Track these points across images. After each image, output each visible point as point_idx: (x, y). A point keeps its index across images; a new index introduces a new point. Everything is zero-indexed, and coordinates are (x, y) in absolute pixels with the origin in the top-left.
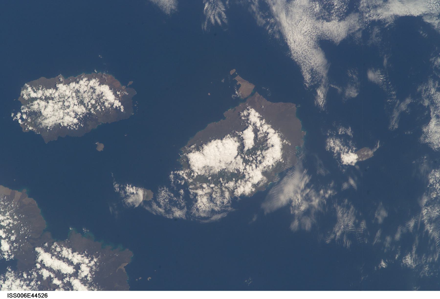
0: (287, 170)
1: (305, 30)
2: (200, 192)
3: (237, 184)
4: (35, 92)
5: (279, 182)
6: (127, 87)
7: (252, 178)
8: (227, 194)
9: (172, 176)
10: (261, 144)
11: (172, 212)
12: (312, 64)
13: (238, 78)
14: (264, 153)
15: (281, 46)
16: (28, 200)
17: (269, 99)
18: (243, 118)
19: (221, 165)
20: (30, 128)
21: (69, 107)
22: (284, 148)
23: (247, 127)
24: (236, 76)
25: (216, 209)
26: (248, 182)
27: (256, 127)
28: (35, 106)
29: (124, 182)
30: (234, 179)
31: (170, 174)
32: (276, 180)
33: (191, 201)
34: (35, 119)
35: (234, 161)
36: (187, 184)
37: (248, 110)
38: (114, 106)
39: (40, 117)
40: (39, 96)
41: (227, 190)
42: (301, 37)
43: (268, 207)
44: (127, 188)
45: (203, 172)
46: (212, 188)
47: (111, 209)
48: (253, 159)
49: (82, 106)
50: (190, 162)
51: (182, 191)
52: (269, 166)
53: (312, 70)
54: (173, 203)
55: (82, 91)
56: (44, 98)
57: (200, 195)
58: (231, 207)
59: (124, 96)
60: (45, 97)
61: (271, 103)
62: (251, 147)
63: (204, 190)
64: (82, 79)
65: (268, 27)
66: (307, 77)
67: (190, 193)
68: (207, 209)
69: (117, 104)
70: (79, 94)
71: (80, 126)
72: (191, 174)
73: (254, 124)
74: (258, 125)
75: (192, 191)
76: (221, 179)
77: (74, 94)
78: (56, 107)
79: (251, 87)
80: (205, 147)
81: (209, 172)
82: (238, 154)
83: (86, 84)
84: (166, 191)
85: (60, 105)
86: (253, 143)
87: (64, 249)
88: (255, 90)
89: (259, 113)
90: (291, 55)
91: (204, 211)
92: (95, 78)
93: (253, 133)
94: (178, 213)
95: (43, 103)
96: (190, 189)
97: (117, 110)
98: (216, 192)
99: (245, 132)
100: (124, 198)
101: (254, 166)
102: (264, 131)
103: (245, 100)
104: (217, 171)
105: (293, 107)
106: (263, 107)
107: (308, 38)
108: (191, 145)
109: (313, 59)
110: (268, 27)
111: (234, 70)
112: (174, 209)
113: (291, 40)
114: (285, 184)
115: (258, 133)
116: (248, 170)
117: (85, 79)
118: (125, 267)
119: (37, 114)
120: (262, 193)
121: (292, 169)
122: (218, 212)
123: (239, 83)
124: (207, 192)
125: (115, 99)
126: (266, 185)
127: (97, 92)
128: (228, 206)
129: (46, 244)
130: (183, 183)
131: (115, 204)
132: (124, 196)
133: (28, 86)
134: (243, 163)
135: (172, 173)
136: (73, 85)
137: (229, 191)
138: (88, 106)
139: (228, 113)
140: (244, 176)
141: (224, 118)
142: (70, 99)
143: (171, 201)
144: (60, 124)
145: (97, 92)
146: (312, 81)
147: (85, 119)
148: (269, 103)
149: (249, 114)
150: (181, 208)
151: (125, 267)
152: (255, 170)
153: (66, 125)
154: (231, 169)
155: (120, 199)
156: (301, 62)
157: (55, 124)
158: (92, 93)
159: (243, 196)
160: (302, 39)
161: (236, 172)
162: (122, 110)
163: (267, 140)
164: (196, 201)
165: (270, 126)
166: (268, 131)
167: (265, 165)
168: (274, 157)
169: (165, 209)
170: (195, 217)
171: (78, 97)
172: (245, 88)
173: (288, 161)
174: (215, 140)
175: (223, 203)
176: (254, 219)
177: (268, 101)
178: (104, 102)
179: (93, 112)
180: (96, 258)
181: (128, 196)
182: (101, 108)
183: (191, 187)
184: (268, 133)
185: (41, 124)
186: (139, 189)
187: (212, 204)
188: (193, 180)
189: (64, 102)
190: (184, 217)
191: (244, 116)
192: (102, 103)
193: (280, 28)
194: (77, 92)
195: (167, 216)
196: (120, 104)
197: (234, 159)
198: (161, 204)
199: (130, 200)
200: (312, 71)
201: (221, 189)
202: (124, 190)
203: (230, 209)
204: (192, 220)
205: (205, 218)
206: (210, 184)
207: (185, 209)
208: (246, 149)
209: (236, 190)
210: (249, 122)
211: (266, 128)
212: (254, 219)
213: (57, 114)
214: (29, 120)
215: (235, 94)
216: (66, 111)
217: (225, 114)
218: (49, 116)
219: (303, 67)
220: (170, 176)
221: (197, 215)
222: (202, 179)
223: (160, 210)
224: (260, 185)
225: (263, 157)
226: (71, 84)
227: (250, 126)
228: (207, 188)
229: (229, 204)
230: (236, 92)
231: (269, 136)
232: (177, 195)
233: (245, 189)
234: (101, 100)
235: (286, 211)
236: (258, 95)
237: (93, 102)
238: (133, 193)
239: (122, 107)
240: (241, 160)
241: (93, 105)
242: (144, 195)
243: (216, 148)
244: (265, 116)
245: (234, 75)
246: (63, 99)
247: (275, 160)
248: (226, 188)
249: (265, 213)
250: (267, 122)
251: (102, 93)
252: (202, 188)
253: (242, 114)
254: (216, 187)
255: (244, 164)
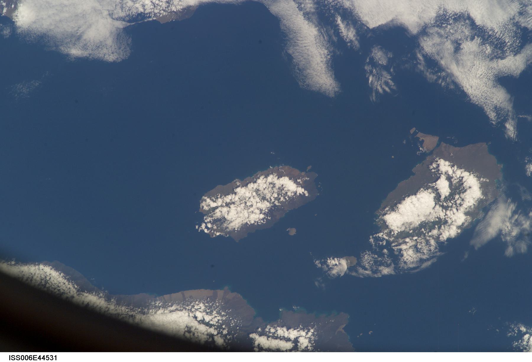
0: (490, 205)
1: (480, 73)
2: (404, 247)
3: (441, 230)
4: (214, 202)
5: (484, 218)
6: (306, 172)
7: (455, 221)
8: (432, 242)
9: (372, 240)
10: (458, 188)
11: (380, 271)
12: (495, 103)
13: (420, 135)
14: (462, 196)
15: (458, 94)
16: (231, 295)
17: (455, 146)
18: (433, 171)
19: (420, 218)
20: (218, 234)
21: (252, 206)
22: (484, 187)
23: (439, 178)
24: (417, 133)
25: (424, 257)
26: (451, 226)
27: (449, 175)
28: (218, 214)
29: (324, 255)
30: (437, 226)
31: (370, 238)
32: (481, 215)
33: (396, 257)
34: (221, 225)
35: (432, 211)
36: (389, 243)
37: (437, 161)
38: (298, 194)
39: (225, 222)
40: (220, 204)
41: (431, 238)
42: (478, 81)
43: (477, 243)
44: (329, 261)
45: (403, 229)
46: (416, 240)
47: (317, 284)
48: (452, 204)
49: (266, 202)
50: (387, 224)
51: (385, 251)
52: (471, 206)
53: (496, 108)
54: (379, 263)
55: (261, 188)
56: (224, 205)
57: (405, 250)
58: (439, 252)
59: (305, 182)
60: (226, 203)
61: (459, 148)
62: (447, 194)
63: (408, 244)
64: (259, 178)
65: (440, 81)
66: (492, 115)
67: (394, 250)
68: (415, 260)
69: (300, 190)
70: (259, 192)
71: (267, 219)
72: (391, 232)
73: (446, 173)
74: (450, 172)
75: (395, 248)
76: (423, 230)
77: (254, 194)
78: (239, 209)
79: (436, 139)
80: (400, 206)
81: (409, 227)
82: (436, 204)
83: (264, 181)
84: (369, 255)
85: (242, 206)
86: (449, 191)
87: (278, 328)
88: (440, 141)
89: (449, 161)
90: (470, 100)
91: (413, 262)
92: (272, 174)
93: (447, 181)
94: (386, 271)
95: (225, 210)
96: (394, 246)
97: (302, 196)
98: (421, 243)
99: (438, 182)
100: (327, 271)
101: (455, 210)
102: (458, 176)
103: (431, 153)
104: (418, 224)
105: (484, 146)
106: (452, 154)
107: (485, 80)
108: (385, 208)
109: (495, 97)
110: (440, 81)
111: (414, 129)
112: (381, 268)
113: (467, 86)
114: (491, 217)
115: (452, 180)
116: (449, 215)
117: (262, 178)
118: (343, 329)
119: (222, 220)
120: (468, 233)
121: (495, 202)
122: (427, 260)
123: (421, 139)
124: (411, 245)
125: (297, 187)
126: (471, 223)
127: (277, 186)
128: (436, 252)
129: (260, 329)
130: (385, 244)
131: (320, 279)
132: (327, 269)
133: (206, 198)
134: (442, 211)
135: (371, 237)
136: (251, 186)
137: (433, 238)
138: (271, 200)
139: (417, 168)
140: (446, 222)
141: (413, 174)
142: (252, 199)
143: (376, 262)
144: (247, 223)
145: (277, 186)
146: (498, 118)
147: (272, 211)
148: (457, 149)
149: (438, 165)
150: (388, 266)
151: (343, 329)
152: (457, 214)
153: (252, 222)
154: (432, 219)
155: (323, 273)
156: (482, 103)
157: (242, 224)
158: (272, 188)
159: (449, 239)
160: (479, 83)
161: (437, 220)
162: (307, 195)
163: (463, 184)
164: (402, 255)
165: (463, 170)
166: (462, 176)
167: (466, 207)
168: (474, 197)
169: (372, 270)
170: (405, 270)
171: (259, 195)
172: (429, 141)
173: (490, 196)
174: (409, 196)
175: (430, 250)
176: (466, 256)
177: (456, 147)
178: (287, 193)
179: (277, 204)
180: (312, 328)
181: (331, 268)
182: (284, 198)
183: (393, 245)
184: (463, 177)
185: (228, 228)
186: (341, 259)
187: (419, 254)
188: (394, 237)
189: (246, 203)
190: (393, 273)
191: (434, 168)
192: (284, 194)
193: (453, 78)
194: (257, 191)
195: (376, 276)
196: (303, 190)
197: (431, 209)
198: (366, 267)
199: (334, 272)
200: (497, 109)
201: (425, 239)
202: (326, 264)
203: (438, 254)
204: (401, 273)
205: (414, 268)
206: (413, 236)
207: (393, 265)
208: (443, 197)
209: (441, 236)
210: (440, 172)
211: (459, 173)
212: (466, 256)
213: (241, 215)
214: (215, 227)
215: (420, 151)
216: (250, 211)
217: (413, 170)
218: (233, 219)
219: (485, 108)
220: (370, 240)
221: (406, 268)
222: (403, 235)
223: (367, 272)
224: (465, 225)
225: (463, 200)
226: (249, 185)
227: (442, 175)
228: (410, 242)
229: (436, 250)
230: (421, 149)
231: (464, 180)
232: (382, 255)
233: (450, 232)
234: (283, 192)
235: (498, 242)
236: (445, 144)
237: (276, 196)
238: (336, 265)
239: (306, 192)
240: (441, 209)
241: (276, 199)
242: (347, 264)
243: (411, 204)
244: (456, 162)
245: (415, 133)
246: (244, 201)
247: (476, 199)
248: (430, 236)
249: (476, 248)
250: (460, 167)
251: (283, 185)
252: (406, 243)
253: (431, 167)
254: (420, 238)
255: (444, 211)
